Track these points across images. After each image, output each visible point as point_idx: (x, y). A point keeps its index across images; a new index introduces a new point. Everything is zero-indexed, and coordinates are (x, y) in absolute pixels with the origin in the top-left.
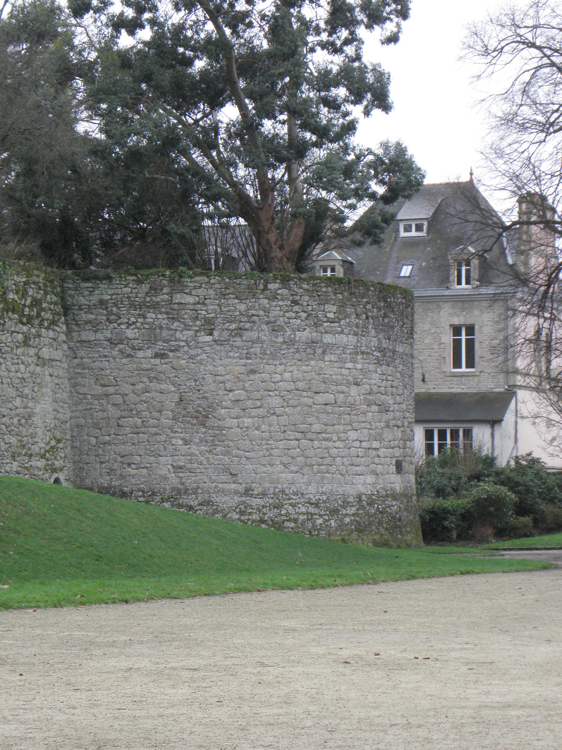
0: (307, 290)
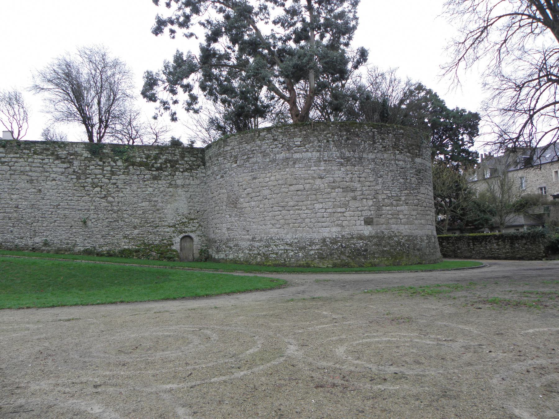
0: (281, 132)
